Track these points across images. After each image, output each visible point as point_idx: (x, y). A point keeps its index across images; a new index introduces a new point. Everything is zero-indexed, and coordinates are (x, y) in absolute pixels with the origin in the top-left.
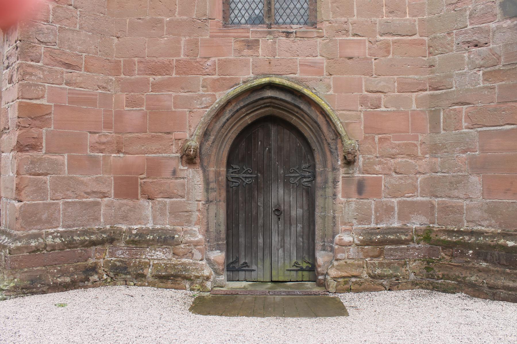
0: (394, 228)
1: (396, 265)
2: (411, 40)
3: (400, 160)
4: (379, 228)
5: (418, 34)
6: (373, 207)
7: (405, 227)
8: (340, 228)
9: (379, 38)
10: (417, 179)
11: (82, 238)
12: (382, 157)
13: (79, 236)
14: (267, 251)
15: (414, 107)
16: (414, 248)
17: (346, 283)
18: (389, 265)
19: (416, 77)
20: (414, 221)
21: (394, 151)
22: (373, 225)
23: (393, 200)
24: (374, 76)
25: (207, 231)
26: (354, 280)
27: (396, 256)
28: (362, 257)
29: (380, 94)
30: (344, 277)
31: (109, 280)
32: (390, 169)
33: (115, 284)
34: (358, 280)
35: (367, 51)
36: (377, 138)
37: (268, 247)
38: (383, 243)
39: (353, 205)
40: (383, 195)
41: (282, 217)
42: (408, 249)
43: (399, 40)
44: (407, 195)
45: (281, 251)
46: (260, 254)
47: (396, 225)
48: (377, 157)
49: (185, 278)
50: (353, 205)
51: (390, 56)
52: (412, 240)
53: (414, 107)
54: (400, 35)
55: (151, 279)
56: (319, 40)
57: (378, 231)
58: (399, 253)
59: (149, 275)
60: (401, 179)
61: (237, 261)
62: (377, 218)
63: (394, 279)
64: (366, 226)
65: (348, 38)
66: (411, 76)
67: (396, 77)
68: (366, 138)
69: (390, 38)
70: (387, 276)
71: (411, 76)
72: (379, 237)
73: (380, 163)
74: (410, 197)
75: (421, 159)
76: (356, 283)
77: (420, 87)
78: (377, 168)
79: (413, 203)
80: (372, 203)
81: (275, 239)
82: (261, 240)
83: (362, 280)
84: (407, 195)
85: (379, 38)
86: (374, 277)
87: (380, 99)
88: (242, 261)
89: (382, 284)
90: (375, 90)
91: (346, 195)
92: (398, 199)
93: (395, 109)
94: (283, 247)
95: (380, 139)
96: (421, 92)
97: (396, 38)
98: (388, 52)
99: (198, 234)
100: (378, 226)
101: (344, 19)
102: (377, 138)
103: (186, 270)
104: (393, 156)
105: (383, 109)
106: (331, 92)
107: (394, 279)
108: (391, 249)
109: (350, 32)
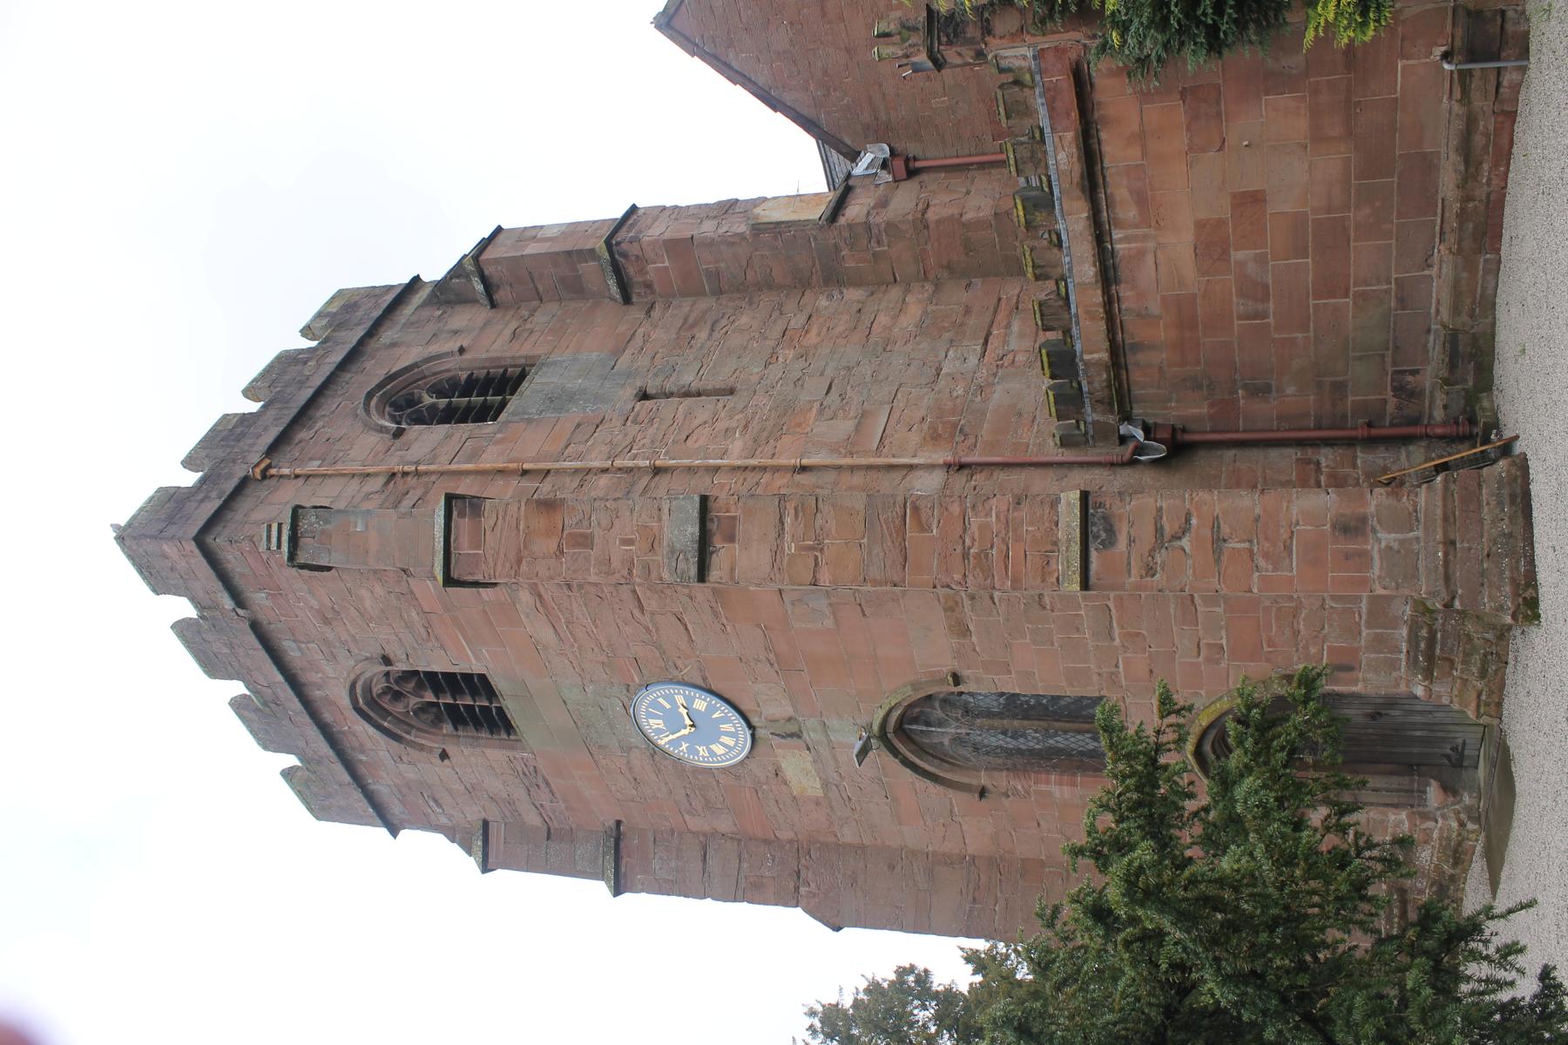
0: (1409, 635)
1: (1467, 646)
2: (1117, 611)
3: (1301, 626)
4: (1408, 652)
5: (1108, 603)
6: (1373, 656)
7: (1409, 622)
8: (1405, 689)
9: (1117, 642)
10: (1332, 607)
11: (1396, 925)
12: (1296, 645)
13: (1392, 927)
14: (1436, 728)
15: (1220, 610)
16: (1443, 625)
17: (1487, 705)
18: (1467, 655)
19: (1173, 606)
20: (1400, 612)
21: (1288, 632)
22: (1403, 656)
23: (1364, 634)
24: (1174, 649)
25: (1396, 806)
26: (1484, 697)
27: (1454, 645)
28: (1450, 679)
29: (1201, 645)
30: (1478, 706)
31: (1455, 905)
32: (1316, 637)
33: (1462, 900)
34: (1484, 693)
35: (1139, 656)
36: (1266, 649)
37: (1428, 726)
38: (1430, 657)
39: (1369, 676)
40: (1356, 645)
41: (1383, 712)
42: (1444, 631)
43: (1118, 623)
44: (1357, 620)
45: (1436, 715)
46: (1440, 734)
47: (1404, 632)
48: (1297, 650)
49: (1459, 844)
50: (1369, 676)
51: (1144, 632)
52: (1430, 627)
53: (1220, 610)
54: (1111, 622)
55: (1458, 871)
56: (1127, 700)
57: (1411, 654)
58: (1450, 642)
59: (1452, 871)
60: (1331, 626)
61: (1448, 757)
62: (1391, 652)
63: (1489, 657)
64: (1404, 663)
65: (1122, 674)
66: (1172, 611)
67: (1175, 628)
68: (1268, 660)
69: (1117, 632)
70: (1483, 666)
71: (1172, 611)
72: (1395, 897)
73: (1306, 647)
74: (1360, 616)
75: (1301, 602)
76: (1489, 696)
77: (1189, 602)
78: (1313, 650)
79: (1370, 613)
80: (1365, 657)
81: (1418, 719)
82: (1418, 733)
83: (1486, 689)
84: (1357, 620)
85: (1117, 642)
86: (1483, 674)
87: (1209, 645)
88: (1449, 751)
89: (1496, 671)
90: (1196, 650)
91: (1355, 682)
92: (1363, 628)
93: (1223, 633)
94: (1430, 712)
95: (1269, 646)
96: (1196, 602)
97: (1115, 624)
98: (1138, 634)
99: (1400, 817)
100: (1405, 650)
101: (1095, 677)
102: (1266, 649)
103: (1449, 839)
104: (1296, 633)
105: (1224, 642)
106: (1203, 692)
107: (1489, 657)
108: (1442, 650)
109: (1114, 670)
